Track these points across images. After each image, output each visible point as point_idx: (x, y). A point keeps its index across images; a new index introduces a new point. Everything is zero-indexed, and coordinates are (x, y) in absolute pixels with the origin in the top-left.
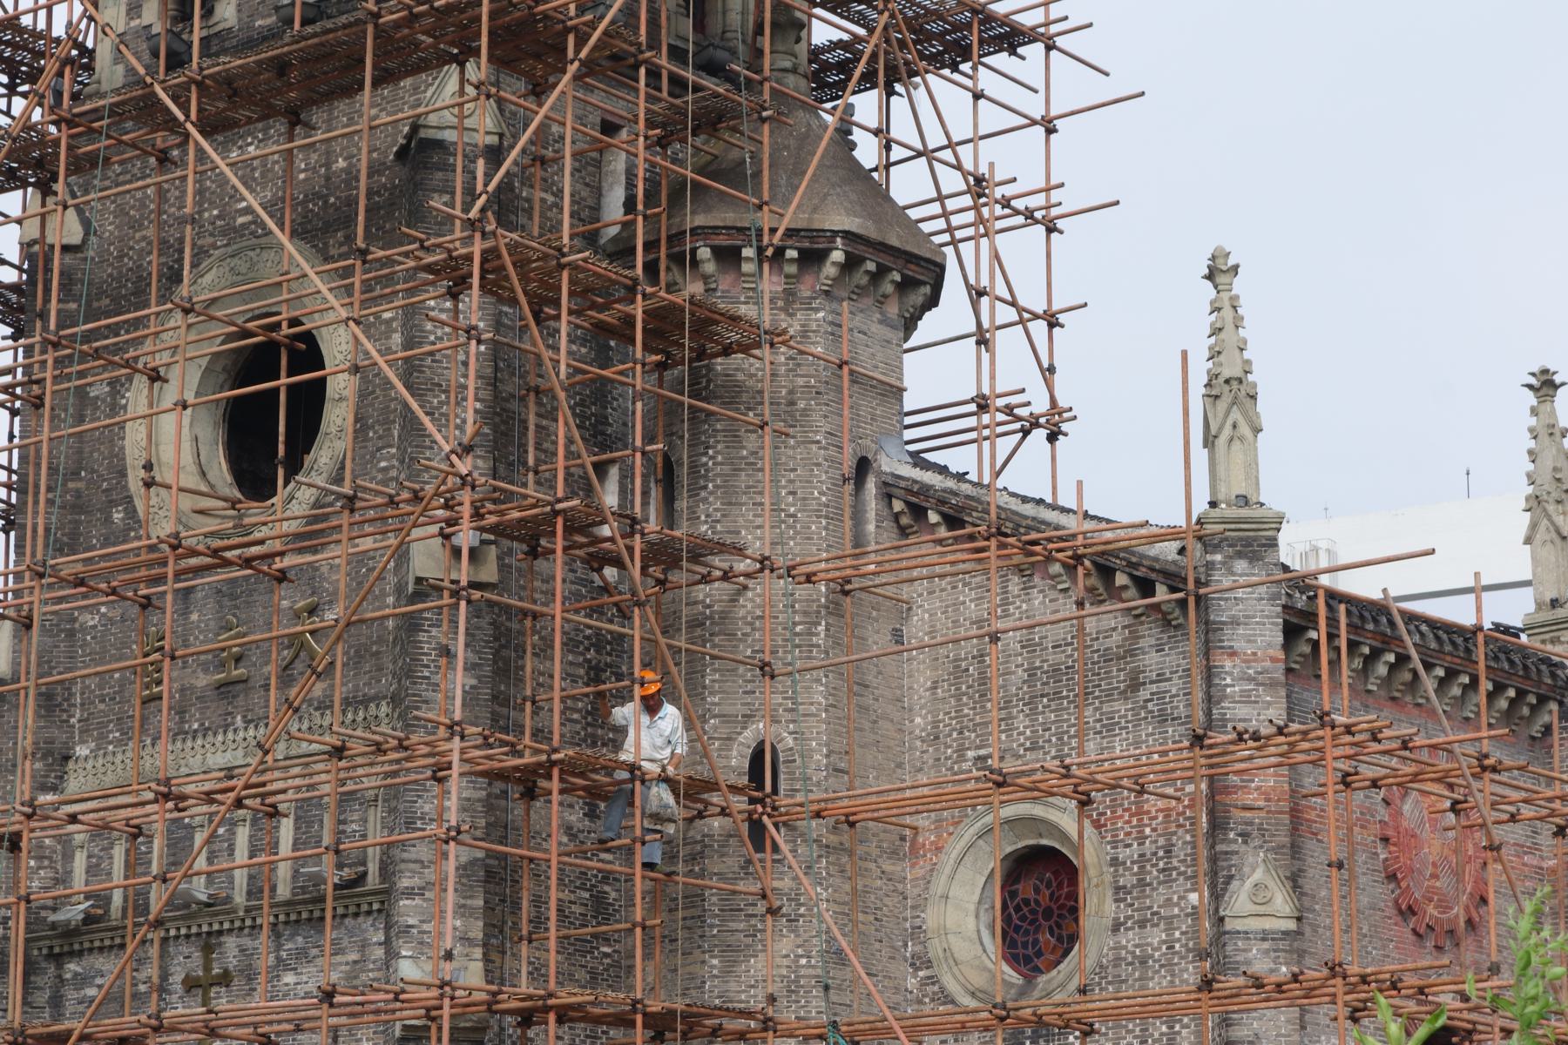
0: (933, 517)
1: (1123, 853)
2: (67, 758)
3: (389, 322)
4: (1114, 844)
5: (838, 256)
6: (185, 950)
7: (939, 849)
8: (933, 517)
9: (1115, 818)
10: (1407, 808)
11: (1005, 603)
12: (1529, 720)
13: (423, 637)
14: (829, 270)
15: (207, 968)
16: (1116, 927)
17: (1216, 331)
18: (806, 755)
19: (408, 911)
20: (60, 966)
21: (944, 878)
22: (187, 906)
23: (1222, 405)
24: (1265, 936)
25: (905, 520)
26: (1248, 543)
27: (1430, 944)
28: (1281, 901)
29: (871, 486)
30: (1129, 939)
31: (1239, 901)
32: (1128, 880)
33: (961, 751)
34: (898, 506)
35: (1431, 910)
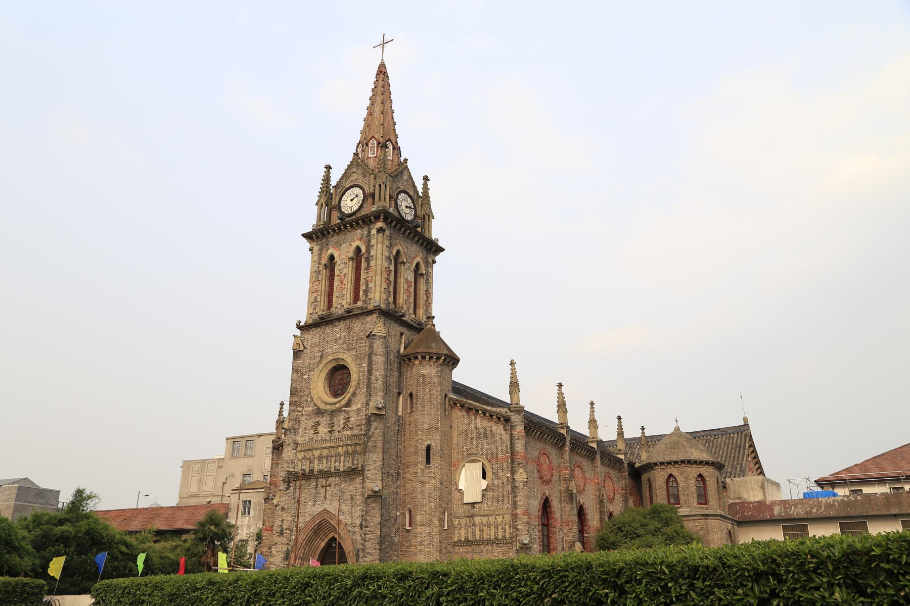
0: (458, 405)
1: (494, 466)
2: (298, 444)
4: (492, 465)
5: (443, 358)
6: (322, 480)
8: (458, 405)
9: (492, 460)
10: (541, 459)
11: (471, 421)
12: (558, 444)
13: (371, 424)
14: (441, 360)
15: (326, 483)
16: (493, 479)
17: (512, 374)
18: (437, 447)
19: (368, 474)
20: (296, 482)
21: (459, 471)
22: (322, 472)
23: (513, 387)
24: (522, 481)
25: (452, 405)
26: (518, 411)
27: (544, 484)
28: (525, 476)
29: (447, 399)
30: (495, 482)
31: (517, 476)
33: (463, 448)
34: (452, 403)
35: (545, 478)
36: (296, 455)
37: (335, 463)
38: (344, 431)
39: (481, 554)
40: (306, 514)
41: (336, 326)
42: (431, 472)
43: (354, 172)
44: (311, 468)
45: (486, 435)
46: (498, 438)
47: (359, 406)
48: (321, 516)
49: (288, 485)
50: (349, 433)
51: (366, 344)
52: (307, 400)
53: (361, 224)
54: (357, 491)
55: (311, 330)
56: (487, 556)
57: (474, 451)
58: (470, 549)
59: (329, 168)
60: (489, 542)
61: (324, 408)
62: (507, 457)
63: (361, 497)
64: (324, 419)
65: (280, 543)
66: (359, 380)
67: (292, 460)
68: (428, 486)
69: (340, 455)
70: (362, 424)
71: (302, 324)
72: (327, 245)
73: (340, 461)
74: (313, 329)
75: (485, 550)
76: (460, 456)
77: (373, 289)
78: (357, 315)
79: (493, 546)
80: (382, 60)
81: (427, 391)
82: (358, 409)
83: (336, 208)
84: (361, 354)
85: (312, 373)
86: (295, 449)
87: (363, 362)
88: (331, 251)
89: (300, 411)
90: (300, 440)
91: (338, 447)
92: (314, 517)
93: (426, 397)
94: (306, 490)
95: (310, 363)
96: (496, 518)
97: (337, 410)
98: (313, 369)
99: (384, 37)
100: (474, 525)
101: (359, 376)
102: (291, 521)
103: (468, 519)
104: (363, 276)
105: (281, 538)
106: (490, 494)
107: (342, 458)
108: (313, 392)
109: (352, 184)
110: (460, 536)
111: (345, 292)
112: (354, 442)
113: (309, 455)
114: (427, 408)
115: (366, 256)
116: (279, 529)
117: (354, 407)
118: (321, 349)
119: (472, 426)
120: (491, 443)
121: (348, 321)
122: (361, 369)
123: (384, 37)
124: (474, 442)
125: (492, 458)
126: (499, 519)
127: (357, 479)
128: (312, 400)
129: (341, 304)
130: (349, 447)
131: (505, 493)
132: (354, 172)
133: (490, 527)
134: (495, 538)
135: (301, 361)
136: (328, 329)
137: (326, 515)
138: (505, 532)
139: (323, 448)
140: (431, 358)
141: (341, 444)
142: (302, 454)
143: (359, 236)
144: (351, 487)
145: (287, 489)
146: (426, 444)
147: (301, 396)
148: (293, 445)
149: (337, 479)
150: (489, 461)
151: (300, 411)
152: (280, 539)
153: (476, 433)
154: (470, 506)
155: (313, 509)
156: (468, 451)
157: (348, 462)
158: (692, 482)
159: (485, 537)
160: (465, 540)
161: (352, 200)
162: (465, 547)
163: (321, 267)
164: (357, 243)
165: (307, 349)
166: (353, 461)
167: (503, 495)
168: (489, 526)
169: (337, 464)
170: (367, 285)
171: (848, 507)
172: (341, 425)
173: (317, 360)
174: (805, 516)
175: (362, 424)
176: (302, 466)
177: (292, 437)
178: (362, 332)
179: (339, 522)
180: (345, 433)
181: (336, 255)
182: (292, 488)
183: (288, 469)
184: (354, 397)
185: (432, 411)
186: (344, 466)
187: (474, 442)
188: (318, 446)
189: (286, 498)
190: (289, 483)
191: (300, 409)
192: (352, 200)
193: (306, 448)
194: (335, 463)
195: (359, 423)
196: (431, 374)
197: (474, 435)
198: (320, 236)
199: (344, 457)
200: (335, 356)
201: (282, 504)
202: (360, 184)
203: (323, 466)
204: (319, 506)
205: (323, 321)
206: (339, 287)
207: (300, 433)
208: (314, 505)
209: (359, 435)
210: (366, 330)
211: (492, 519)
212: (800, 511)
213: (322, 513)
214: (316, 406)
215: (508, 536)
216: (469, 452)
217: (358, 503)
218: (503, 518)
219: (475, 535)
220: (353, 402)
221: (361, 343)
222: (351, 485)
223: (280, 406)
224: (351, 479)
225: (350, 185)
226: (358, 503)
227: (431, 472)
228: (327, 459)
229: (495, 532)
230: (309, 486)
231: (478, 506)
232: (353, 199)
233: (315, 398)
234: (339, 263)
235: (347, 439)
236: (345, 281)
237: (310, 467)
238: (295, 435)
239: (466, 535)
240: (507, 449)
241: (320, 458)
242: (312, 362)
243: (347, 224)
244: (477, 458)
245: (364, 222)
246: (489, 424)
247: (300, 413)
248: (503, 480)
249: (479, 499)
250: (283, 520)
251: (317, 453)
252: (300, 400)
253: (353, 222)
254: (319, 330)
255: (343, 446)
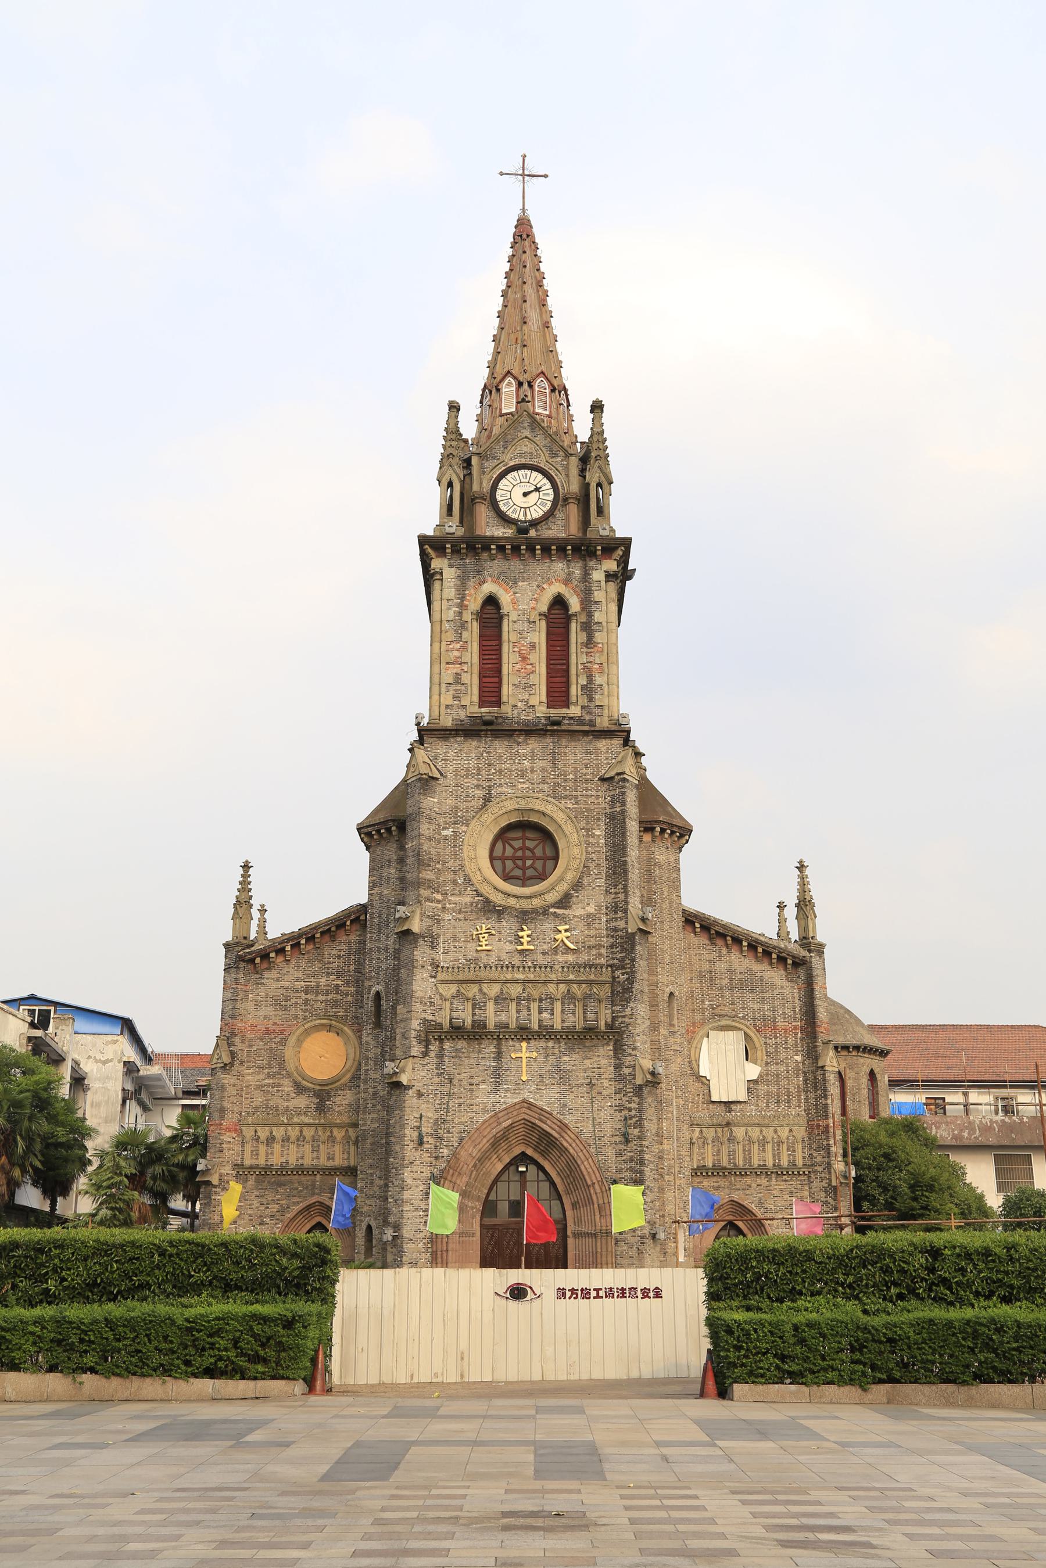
2: (438, 966)
3: (599, 836)
6: (511, 1043)
7: (694, 1032)
9: (765, 1030)
11: (720, 956)
16: (767, 1064)
30: (773, 1068)
32: (771, 1050)
33: (703, 1002)
36: (437, 989)
37: (540, 1012)
38: (556, 954)
39: (748, 1192)
40: (475, 1108)
41: (519, 744)
42: (676, 1043)
43: (526, 437)
44: (476, 1018)
45: (751, 985)
46: (776, 992)
47: (591, 909)
48: (515, 1113)
49: (427, 1047)
50: (571, 958)
51: (599, 793)
52: (455, 882)
53: (570, 552)
54: (602, 1070)
55: (452, 740)
56: (759, 1195)
57: (727, 1010)
58: (722, 1182)
59: (454, 408)
60: (763, 1171)
61: (503, 903)
62: (796, 1028)
63: (612, 1083)
64: (504, 923)
65: (418, 1163)
66: (587, 859)
67: (430, 997)
68: (674, 1067)
69: (552, 999)
70: (600, 946)
71: (425, 722)
72: (479, 572)
73: (552, 1010)
74: (459, 739)
75: (754, 1185)
76: (698, 1018)
77: (605, 687)
78: (573, 734)
79: (771, 1178)
80: (523, 210)
81: (666, 893)
82: (589, 915)
83: (485, 500)
84: (587, 810)
85: (464, 828)
86: (435, 977)
87: (595, 826)
88: (489, 588)
89: (438, 902)
90: (443, 960)
91: (545, 982)
92: (496, 1114)
93: (664, 906)
94: (472, 1061)
95: (457, 808)
96: (776, 1132)
97: (535, 911)
98: (467, 820)
99: (524, 160)
100: (732, 1139)
101: (587, 852)
102: (436, 1120)
103: (719, 1130)
104: (577, 658)
105: (420, 1153)
106: (763, 1088)
107: (558, 1006)
108: (470, 868)
109: (523, 461)
110: (703, 1159)
111: (534, 679)
112: (584, 978)
113: (473, 990)
114: (666, 926)
115: (583, 618)
116: (415, 1134)
117: (577, 911)
118: (485, 784)
119: (721, 966)
120: (763, 1000)
121: (549, 739)
122: (591, 840)
123: (524, 160)
124: (727, 994)
125: (765, 1025)
126: (784, 1133)
127: (601, 1049)
128: (468, 881)
129: (527, 702)
130: (575, 986)
131: (792, 1089)
132: (526, 437)
133: (764, 1146)
134: (774, 1165)
135: (436, 800)
136: (500, 747)
137: (528, 1112)
138: (794, 1157)
139: (506, 982)
140: (673, 833)
141: (553, 977)
142: (453, 989)
143: (563, 575)
144: (586, 1061)
145: (425, 1054)
146: (668, 990)
147: (439, 870)
148: (429, 968)
149: (551, 1044)
150: (758, 1031)
151: (438, 902)
152: (418, 1154)
153: (731, 979)
154: (722, 1106)
155: (493, 1098)
156: (713, 1009)
157: (574, 1013)
158: (865, 1080)
159: (756, 1163)
160: (714, 1166)
161: (525, 494)
162: (715, 1179)
163: (467, 616)
164: (556, 588)
165: (445, 777)
166: (584, 1013)
167: (788, 1092)
168: (763, 1143)
169: (545, 1015)
170: (590, 678)
171: (1012, 1132)
172: (547, 940)
173: (477, 803)
174: (954, 1143)
175: (600, 946)
176: (451, 1010)
177: (428, 951)
178: (586, 767)
179: (563, 1127)
180: (560, 958)
181: (505, 599)
182: (432, 1054)
183: (424, 1015)
184: (577, 891)
185: (673, 931)
186: (563, 1021)
187: (727, 994)
188: (493, 974)
189: (424, 1074)
190: (427, 1043)
191: (439, 897)
192: (525, 494)
193: (461, 977)
194: (540, 1012)
195: (593, 942)
196: (669, 863)
197: (725, 982)
198: (463, 551)
199: (563, 1003)
200: (523, 804)
201: (418, 1085)
202: (541, 465)
203: (511, 1017)
204: (509, 1094)
205: (489, 728)
206: (518, 666)
207: (441, 945)
208: (496, 1091)
209: (596, 966)
210: (597, 765)
211: (769, 1133)
212: (945, 1134)
213: (517, 1107)
214: (479, 894)
215: (800, 1163)
216: (717, 1011)
217: (605, 1093)
218: (791, 1130)
219: (734, 1159)
220: (574, 899)
221: (587, 789)
222: (586, 1058)
223: (241, 871)
224: (585, 1047)
225: (517, 461)
226: (605, 1093)
227: (676, 1043)
228: (518, 1004)
229: (774, 1155)
230: (480, 1052)
231: (739, 1107)
232: (530, 492)
233: (476, 878)
234: (513, 616)
235: (565, 969)
236: (533, 658)
237: (474, 1015)
238: (433, 948)
239: (716, 1158)
240: (794, 1011)
241: (501, 1000)
242: (462, 806)
243: (538, 544)
244: (734, 1024)
245: (576, 549)
246: (757, 967)
247: (440, 906)
248: (787, 1066)
249: (742, 1096)
250: (421, 1116)
251: (494, 990)
252: (437, 878)
253: (553, 544)
254: (475, 743)
255: (559, 982)
